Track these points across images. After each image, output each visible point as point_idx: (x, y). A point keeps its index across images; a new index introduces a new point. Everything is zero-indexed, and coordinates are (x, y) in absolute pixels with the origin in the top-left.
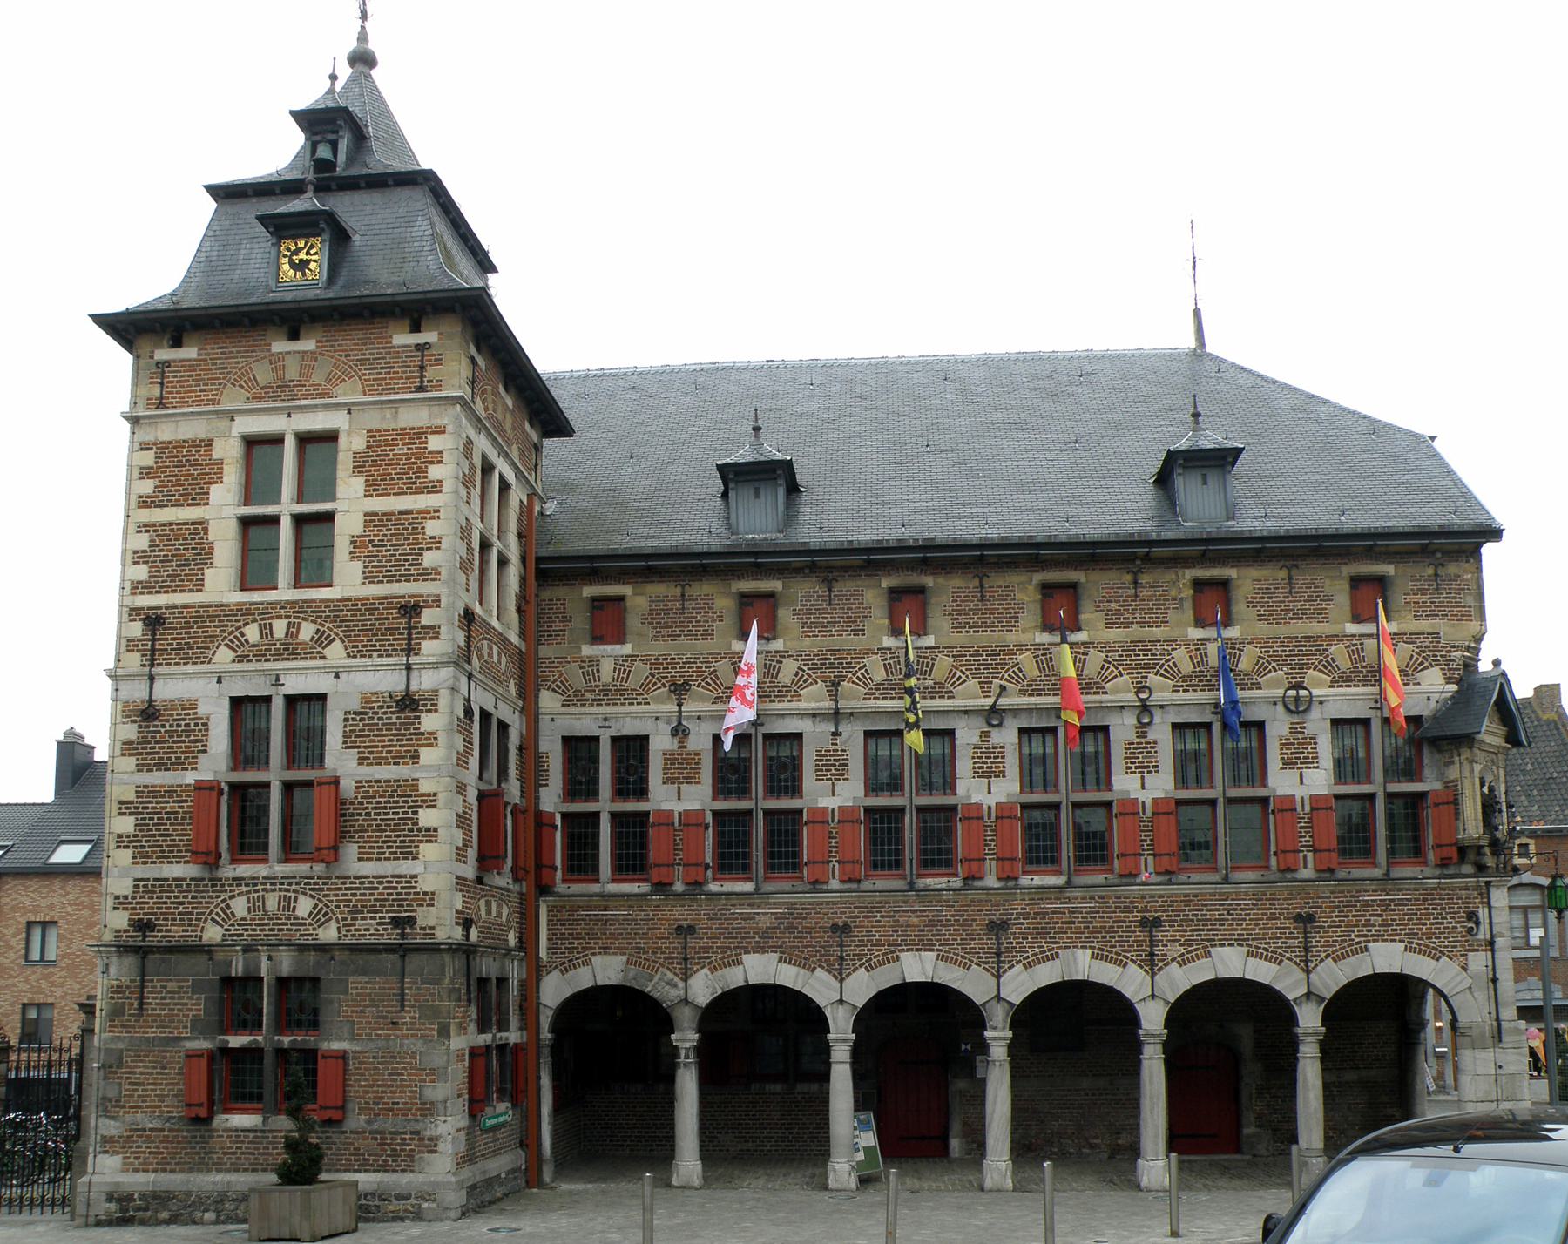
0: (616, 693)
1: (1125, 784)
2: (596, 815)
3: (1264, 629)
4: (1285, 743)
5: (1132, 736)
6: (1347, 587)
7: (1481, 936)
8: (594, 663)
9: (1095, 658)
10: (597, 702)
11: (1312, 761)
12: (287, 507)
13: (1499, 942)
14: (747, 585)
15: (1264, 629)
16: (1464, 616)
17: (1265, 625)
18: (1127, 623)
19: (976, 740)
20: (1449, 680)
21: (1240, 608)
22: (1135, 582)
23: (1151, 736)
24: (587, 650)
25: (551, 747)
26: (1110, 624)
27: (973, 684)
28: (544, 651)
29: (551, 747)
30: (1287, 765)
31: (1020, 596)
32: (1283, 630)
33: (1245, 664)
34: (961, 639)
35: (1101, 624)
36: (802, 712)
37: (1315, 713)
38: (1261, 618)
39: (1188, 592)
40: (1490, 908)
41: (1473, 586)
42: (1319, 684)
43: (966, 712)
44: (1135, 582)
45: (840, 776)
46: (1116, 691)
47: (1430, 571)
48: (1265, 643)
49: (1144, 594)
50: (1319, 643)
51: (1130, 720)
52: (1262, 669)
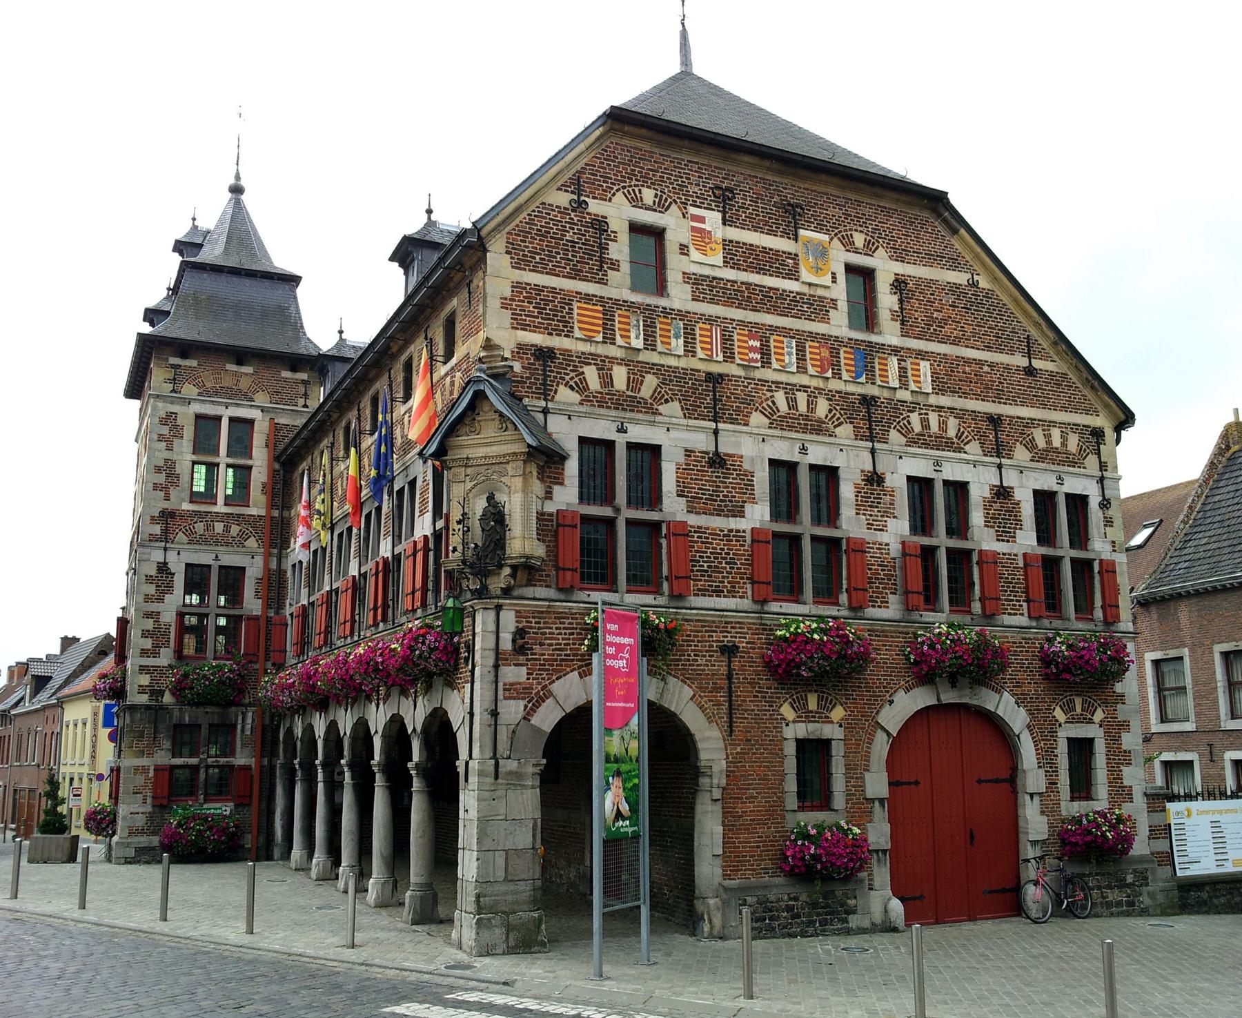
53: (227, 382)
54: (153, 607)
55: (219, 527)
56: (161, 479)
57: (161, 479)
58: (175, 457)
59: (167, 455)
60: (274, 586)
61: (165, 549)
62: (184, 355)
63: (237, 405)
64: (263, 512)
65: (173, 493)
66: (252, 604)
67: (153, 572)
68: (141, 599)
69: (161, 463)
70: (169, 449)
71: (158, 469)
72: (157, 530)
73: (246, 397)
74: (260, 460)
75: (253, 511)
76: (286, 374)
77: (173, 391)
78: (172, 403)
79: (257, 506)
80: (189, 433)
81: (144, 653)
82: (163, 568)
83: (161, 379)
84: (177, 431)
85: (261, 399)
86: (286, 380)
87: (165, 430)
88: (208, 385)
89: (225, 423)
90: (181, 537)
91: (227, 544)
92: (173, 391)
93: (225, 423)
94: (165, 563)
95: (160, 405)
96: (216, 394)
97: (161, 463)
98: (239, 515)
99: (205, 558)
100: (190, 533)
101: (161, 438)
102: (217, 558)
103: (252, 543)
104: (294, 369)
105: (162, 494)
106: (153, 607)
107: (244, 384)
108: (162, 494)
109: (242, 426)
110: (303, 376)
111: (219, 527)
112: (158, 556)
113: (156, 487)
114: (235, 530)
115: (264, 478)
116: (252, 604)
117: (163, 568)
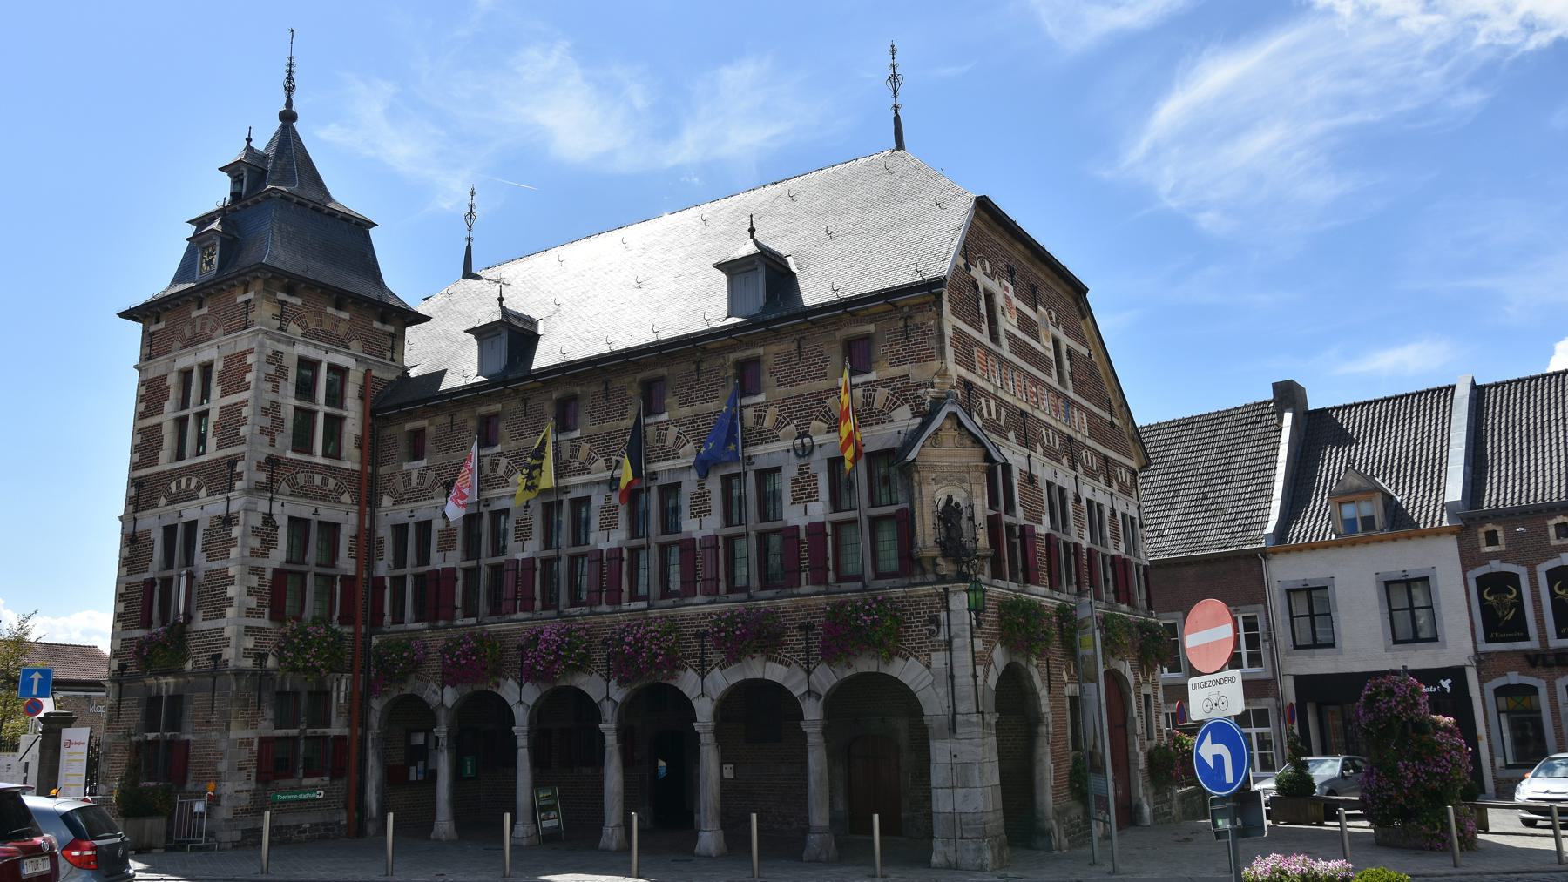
0: (420, 494)
1: (690, 526)
2: (404, 577)
3: (781, 392)
4: (795, 482)
5: (696, 489)
6: (839, 348)
7: (941, 638)
8: (408, 474)
9: (673, 431)
10: (409, 500)
11: (813, 496)
12: (190, 412)
13: (957, 642)
14: (484, 410)
15: (781, 392)
16: (929, 358)
17: (782, 389)
18: (692, 403)
19: (602, 503)
20: (915, 415)
21: (767, 379)
22: (698, 369)
23: (707, 487)
24: (406, 466)
25: (385, 533)
26: (682, 404)
27: (601, 462)
28: (382, 470)
29: (385, 533)
30: (796, 500)
31: (630, 393)
32: (794, 390)
33: (767, 423)
34: (594, 429)
35: (676, 406)
36: (513, 494)
37: (817, 455)
38: (780, 384)
39: (731, 372)
40: (948, 610)
41: (935, 330)
42: (819, 432)
43: (598, 483)
44: (698, 369)
45: (528, 537)
46: (685, 456)
47: (901, 324)
48: (781, 404)
49: (704, 378)
50: (819, 398)
51: (694, 475)
52: (779, 424)
53: (327, 327)
54: (259, 562)
55: (318, 479)
56: (267, 422)
57: (267, 422)
58: (280, 400)
59: (272, 396)
60: (366, 544)
61: (271, 499)
62: (290, 291)
63: (336, 351)
64: (356, 467)
65: (278, 439)
66: (346, 563)
67: (259, 524)
68: (247, 553)
69: (268, 405)
70: (275, 390)
71: (265, 412)
72: (262, 477)
73: (342, 344)
74: (353, 412)
75: (348, 465)
76: (377, 325)
77: (281, 328)
78: (279, 341)
79: (351, 460)
80: (292, 375)
81: (250, 613)
82: (268, 519)
83: (269, 314)
84: (282, 372)
85: (356, 347)
86: (377, 331)
87: (272, 370)
88: (312, 326)
89: (323, 369)
90: (285, 488)
91: (324, 499)
92: (281, 328)
93: (323, 369)
94: (270, 515)
95: (268, 342)
96: (317, 337)
97: (268, 405)
98: (335, 468)
99: (304, 510)
100: (292, 484)
101: (268, 378)
102: (316, 513)
103: (346, 498)
104: (383, 321)
105: (267, 439)
106: (259, 562)
107: (342, 330)
108: (267, 439)
109: (338, 371)
110: (390, 329)
111: (318, 479)
112: (263, 506)
113: (263, 431)
114: (332, 483)
115: (358, 432)
116: (346, 563)
117: (268, 519)
